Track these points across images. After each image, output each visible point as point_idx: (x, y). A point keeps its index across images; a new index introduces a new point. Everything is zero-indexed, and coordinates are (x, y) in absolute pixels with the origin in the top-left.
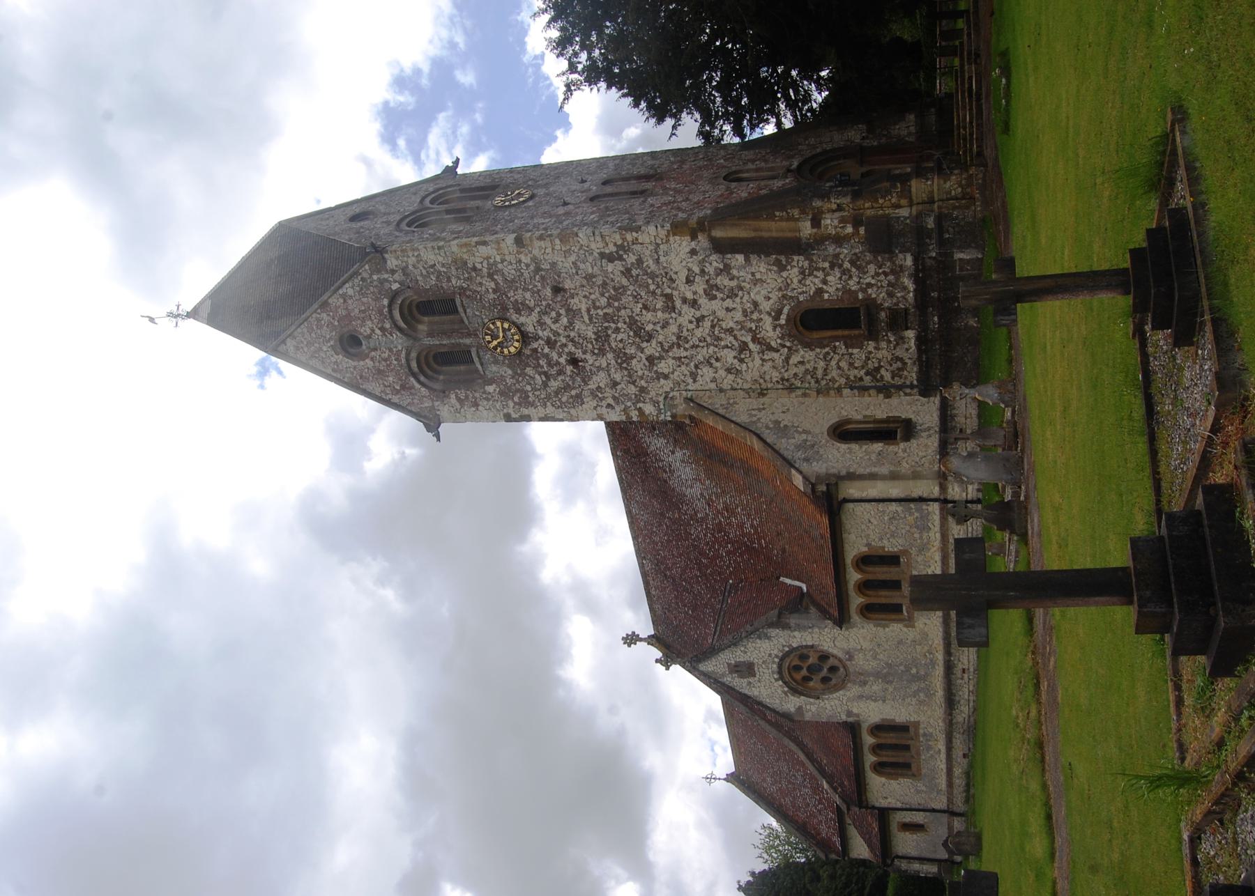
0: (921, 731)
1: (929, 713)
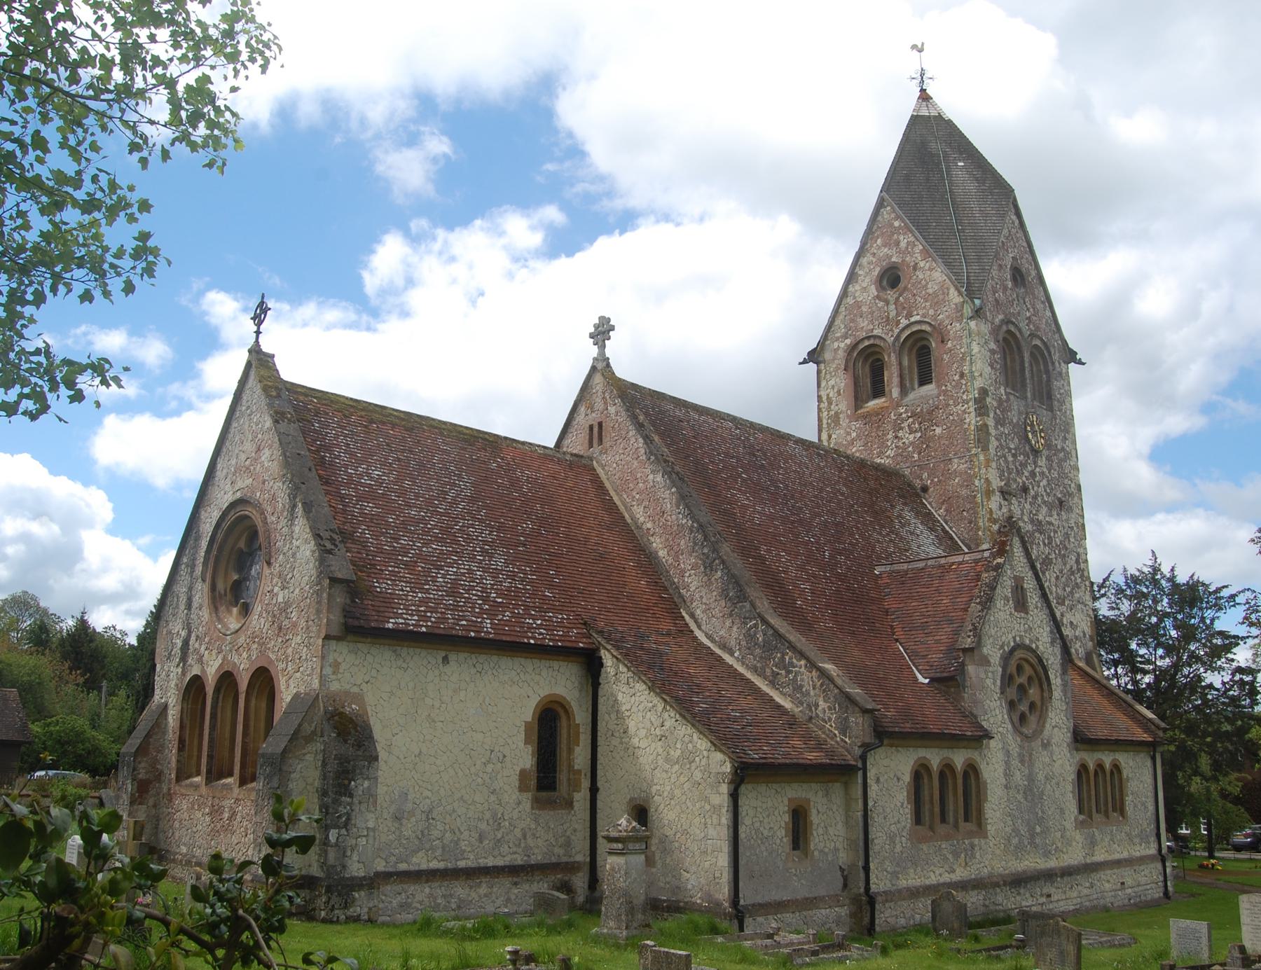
0: (976, 841)
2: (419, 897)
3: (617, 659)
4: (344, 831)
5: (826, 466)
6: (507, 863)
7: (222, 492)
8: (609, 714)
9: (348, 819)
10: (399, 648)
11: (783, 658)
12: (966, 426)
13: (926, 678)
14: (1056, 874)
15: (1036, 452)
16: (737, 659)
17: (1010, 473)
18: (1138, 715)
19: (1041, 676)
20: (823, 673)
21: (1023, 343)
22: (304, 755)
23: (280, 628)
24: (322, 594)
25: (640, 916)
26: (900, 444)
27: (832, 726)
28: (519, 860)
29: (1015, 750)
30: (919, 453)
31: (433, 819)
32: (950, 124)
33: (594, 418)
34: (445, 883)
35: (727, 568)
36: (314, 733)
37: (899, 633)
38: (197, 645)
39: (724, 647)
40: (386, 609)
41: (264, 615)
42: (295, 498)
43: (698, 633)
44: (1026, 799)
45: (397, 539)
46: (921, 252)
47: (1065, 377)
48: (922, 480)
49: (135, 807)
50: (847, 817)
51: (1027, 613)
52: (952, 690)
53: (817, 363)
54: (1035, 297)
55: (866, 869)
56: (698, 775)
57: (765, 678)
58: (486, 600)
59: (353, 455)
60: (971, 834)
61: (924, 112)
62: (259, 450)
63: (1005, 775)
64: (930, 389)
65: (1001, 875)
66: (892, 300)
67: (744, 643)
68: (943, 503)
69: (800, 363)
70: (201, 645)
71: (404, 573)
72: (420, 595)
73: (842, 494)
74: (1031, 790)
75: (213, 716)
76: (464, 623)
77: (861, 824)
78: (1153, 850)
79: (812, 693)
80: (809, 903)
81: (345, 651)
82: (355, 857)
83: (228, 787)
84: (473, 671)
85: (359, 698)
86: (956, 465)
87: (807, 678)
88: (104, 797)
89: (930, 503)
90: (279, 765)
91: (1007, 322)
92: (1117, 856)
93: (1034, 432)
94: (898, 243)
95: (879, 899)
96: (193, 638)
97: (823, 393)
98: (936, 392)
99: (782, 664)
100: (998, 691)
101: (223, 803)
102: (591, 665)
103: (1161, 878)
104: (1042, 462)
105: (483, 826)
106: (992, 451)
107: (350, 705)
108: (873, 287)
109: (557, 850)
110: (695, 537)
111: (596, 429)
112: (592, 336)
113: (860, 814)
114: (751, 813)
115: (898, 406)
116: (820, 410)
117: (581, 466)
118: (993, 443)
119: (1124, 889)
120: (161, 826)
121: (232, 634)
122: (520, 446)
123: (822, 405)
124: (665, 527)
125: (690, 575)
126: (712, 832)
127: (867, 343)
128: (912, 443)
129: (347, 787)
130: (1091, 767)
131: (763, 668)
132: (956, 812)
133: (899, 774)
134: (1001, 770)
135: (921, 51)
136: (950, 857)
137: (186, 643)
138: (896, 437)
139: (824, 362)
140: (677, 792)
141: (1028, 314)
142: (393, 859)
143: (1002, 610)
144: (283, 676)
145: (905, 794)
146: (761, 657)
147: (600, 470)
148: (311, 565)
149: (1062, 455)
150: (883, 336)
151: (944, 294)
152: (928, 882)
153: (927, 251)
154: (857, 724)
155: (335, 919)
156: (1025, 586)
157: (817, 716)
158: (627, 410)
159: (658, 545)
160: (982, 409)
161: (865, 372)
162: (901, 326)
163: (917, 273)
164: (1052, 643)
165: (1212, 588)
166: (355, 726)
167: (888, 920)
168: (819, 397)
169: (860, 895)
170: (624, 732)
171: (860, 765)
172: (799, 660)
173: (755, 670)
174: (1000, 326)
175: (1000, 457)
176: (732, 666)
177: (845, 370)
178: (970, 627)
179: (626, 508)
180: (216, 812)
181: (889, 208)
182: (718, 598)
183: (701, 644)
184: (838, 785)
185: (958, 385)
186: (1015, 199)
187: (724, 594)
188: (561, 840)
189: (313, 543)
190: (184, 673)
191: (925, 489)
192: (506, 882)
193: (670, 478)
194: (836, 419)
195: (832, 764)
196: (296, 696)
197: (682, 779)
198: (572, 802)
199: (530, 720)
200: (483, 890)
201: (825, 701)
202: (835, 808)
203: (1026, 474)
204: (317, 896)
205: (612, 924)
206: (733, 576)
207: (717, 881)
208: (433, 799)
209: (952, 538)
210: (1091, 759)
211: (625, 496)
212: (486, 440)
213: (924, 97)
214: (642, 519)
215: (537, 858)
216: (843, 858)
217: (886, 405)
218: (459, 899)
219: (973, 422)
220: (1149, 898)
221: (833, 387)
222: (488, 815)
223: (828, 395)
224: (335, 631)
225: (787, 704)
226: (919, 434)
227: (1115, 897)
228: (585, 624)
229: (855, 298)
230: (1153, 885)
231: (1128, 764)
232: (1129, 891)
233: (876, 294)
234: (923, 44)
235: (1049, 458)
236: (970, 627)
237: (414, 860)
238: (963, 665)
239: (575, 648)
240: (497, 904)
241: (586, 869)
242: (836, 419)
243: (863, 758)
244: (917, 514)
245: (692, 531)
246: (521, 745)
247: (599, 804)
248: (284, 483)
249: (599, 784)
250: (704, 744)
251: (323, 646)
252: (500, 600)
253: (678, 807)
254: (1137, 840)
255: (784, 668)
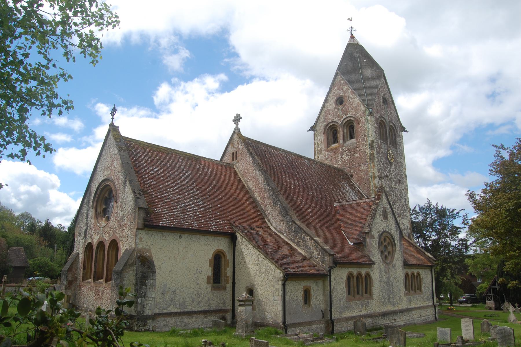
0: (369, 301)
1: (377, 304)
2: (171, 322)
3: (242, 236)
4: (143, 299)
5: (317, 168)
6: (203, 310)
7: (100, 176)
8: (239, 256)
9: (145, 294)
10: (164, 233)
11: (301, 236)
12: (366, 154)
13: (352, 243)
14: (397, 312)
15: (391, 163)
16: (285, 236)
17: (382, 171)
18: (426, 256)
19: (392, 243)
20: (316, 241)
21: (386, 125)
22: (129, 271)
23: (121, 225)
24: (136, 213)
25: (250, 328)
26: (343, 160)
27: (318, 260)
28: (207, 308)
29: (383, 268)
30: (350, 163)
31: (176, 294)
32: (361, 46)
33: (234, 150)
34: (180, 317)
35: (281, 204)
36: (133, 263)
37: (342, 227)
38: (90, 232)
39: (280, 232)
40: (159, 219)
41: (115, 221)
42: (126, 178)
43: (271, 227)
44: (387, 286)
45: (163, 193)
46: (351, 92)
47: (401, 137)
48: (351, 173)
49: (67, 290)
50: (324, 292)
51: (387, 220)
52: (361, 247)
53: (314, 131)
54: (390, 108)
55: (331, 311)
56: (271, 278)
57: (295, 243)
58: (195, 215)
59: (147, 163)
60: (367, 298)
61: (352, 42)
62: (113, 161)
63: (380, 277)
64: (354, 140)
65: (378, 313)
66: (340, 109)
67: (287, 231)
68: (358, 181)
69: (308, 131)
70: (91, 231)
71: (165, 205)
72: (171, 213)
73: (323, 178)
74: (389, 283)
75: (96, 257)
76: (187, 223)
77: (329, 295)
78: (431, 304)
79: (312, 248)
80: (310, 323)
81: (144, 234)
82: (148, 308)
83: (101, 283)
84: (191, 241)
85: (149, 251)
86: (362, 167)
87: (310, 243)
88: (56, 287)
89: (354, 181)
90: (120, 275)
91: (381, 117)
92: (419, 306)
93: (390, 156)
94: (343, 89)
95: (335, 321)
96: (89, 229)
97: (316, 142)
98: (356, 141)
99: (301, 238)
100: (377, 247)
101: (100, 289)
102: (233, 239)
103: (434, 313)
104: (393, 166)
105: (194, 296)
106: (375, 162)
107: (146, 253)
108: (334, 104)
109: (220, 305)
110: (270, 193)
111: (235, 154)
112: (233, 121)
113: (328, 291)
114: (290, 291)
115: (342, 146)
116: (315, 148)
117: (229, 167)
118: (376, 160)
119: (421, 317)
120: (77, 297)
121: (103, 227)
122: (207, 160)
123: (315, 146)
124: (259, 189)
125: (268, 206)
126: (276, 298)
127: (331, 124)
128: (347, 160)
129: (145, 283)
130: (410, 274)
131: (294, 240)
132: (362, 290)
133: (342, 277)
134: (378, 276)
135: (351, 20)
136: (360, 306)
137: (86, 231)
138: (342, 157)
139: (316, 130)
140: (264, 284)
141: (388, 114)
142: (161, 308)
143: (379, 219)
144: (122, 243)
145: (344, 284)
146: (293, 236)
147: (236, 169)
148: (132, 203)
149: (400, 164)
150: (337, 121)
151: (359, 107)
152: (352, 315)
153: (353, 92)
154: (327, 259)
155: (140, 330)
156: (387, 210)
157: (313, 256)
158: (246, 147)
159: (257, 195)
160: (372, 148)
161: (331, 134)
162: (344, 118)
163: (350, 99)
164: (396, 230)
165: (451, 210)
166: (148, 260)
167: (338, 329)
168: (315, 143)
169: (328, 320)
170: (245, 263)
171: (328, 274)
172: (307, 237)
173: (291, 240)
174: (378, 119)
175: (378, 165)
176: (283, 239)
177: (324, 133)
178: (368, 225)
179: (245, 182)
180: (97, 292)
181: (339, 76)
182: (278, 214)
183: (272, 231)
184: (320, 281)
185: (364, 139)
186: (384, 74)
187: (281, 213)
188: (222, 301)
189: (132, 195)
190: (85, 242)
191: (352, 176)
192: (202, 316)
193: (261, 172)
194: (320, 151)
195: (318, 274)
196: (126, 250)
197: (265, 279)
198: (226, 288)
199: (211, 258)
200: (194, 319)
201: (316, 251)
202: (319, 289)
203: (387, 171)
204: (133, 322)
205: (240, 331)
206: (284, 207)
207: (278, 315)
208: (176, 287)
209: (361, 193)
210: (410, 271)
211: (245, 178)
212: (195, 158)
213: (352, 37)
214: (251, 186)
215: (213, 308)
216: (323, 307)
217: (338, 146)
218: (185, 322)
219: (369, 152)
220: (430, 320)
221: (319, 139)
222: (196, 292)
224: (141, 226)
225: (303, 252)
226: (350, 157)
227: (418, 320)
228: (231, 224)
229: (327, 108)
230: (431, 316)
231: (422, 273)
232: (423, 318)
233: (335, 106)
234: (352, 18)
235: (395, 165)
236: (368, 225)
237: (169, 309)
238: (365, 238)
239: (227, 233)
240: (199, 325)
241: (231, 311)
242: (320, 151)
243: (330, 271)
244: (349, 185)
245: (269, 191)
246: (208, 267)
247: (236, 288)
248: (122, 173)
249: (236, 281)
250: (273, 267)
251: (136, 232)
252: (200, 215)
253: (264, 289)
254: (426, 300)
255: (302, 240)
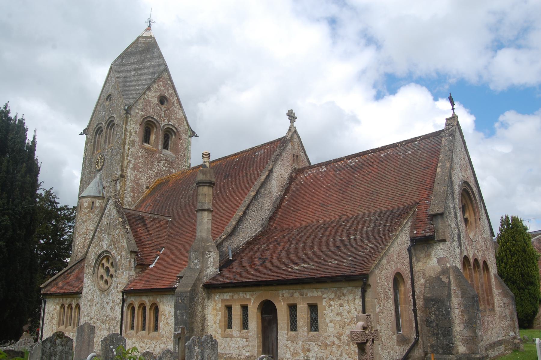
128: (164, 171)
177: (140, 125)
223: (130, 130)
226: (167, 169)
229: (148, 97)
